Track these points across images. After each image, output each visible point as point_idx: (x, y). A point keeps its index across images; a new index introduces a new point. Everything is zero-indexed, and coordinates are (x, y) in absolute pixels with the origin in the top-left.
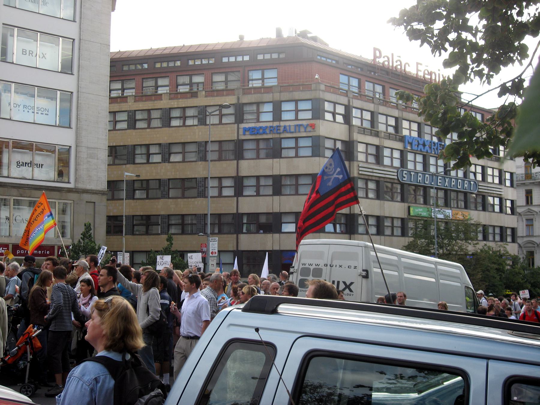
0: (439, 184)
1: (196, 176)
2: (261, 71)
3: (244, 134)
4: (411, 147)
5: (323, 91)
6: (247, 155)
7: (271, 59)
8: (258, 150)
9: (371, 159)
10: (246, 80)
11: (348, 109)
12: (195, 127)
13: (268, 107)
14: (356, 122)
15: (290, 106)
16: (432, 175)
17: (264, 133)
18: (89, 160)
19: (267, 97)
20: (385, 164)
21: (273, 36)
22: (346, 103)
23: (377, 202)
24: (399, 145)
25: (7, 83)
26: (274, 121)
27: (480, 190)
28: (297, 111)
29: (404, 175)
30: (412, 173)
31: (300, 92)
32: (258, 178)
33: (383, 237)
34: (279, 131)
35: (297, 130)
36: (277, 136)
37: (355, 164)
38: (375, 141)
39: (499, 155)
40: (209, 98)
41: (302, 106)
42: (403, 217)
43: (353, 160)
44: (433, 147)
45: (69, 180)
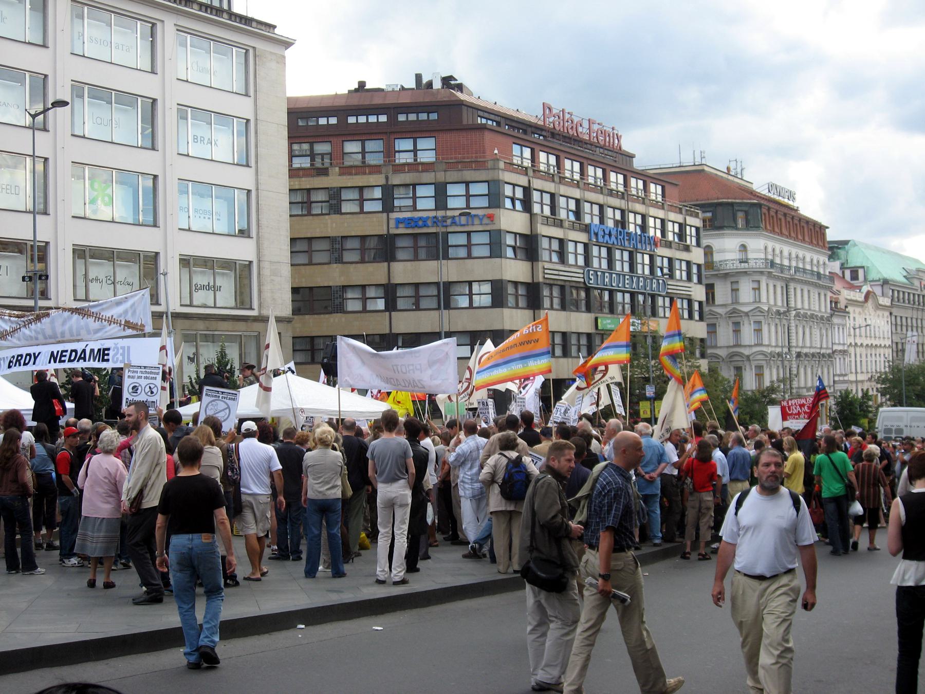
0: (627, 286)
1: (331, 284)
2: (412, 140)
3: (397, 228)
4: (597, 239)
5: (502, 170)
6: (400, 255)
7: (418, 121)
8: (416, 248)
9: (555, 258)
10: (390, 152)
11: (527, 191)
12: (327, 217)
13: (430, 191)
14: (536, 209)
15: (459, 190)
16: (618, 275)
17: (425, 226)
18: (272, 277)
19: (428, 177)
20: (570, 263)
21: (411, 84)
22: (526, 185)
23: (563, 313)
24: (582, 237)
25: (184, 182)
26: (437, 209)
27: (669, 291)
28: (468, 196)
29: (591, 277)
30: (599, 273)
31: (473, 171)
32: (417, 285)
33: (570, 360)
34: (445, 224)
35: (470, 222)
36: (444, 230)
37: (540, 264)
38: (557, 232)
39: (686, 241)
40: (345, 177)
41: (475, 189)
42: (590, 331)
43: (537, 260)
44: (619, 237)
45: (251, 306)
